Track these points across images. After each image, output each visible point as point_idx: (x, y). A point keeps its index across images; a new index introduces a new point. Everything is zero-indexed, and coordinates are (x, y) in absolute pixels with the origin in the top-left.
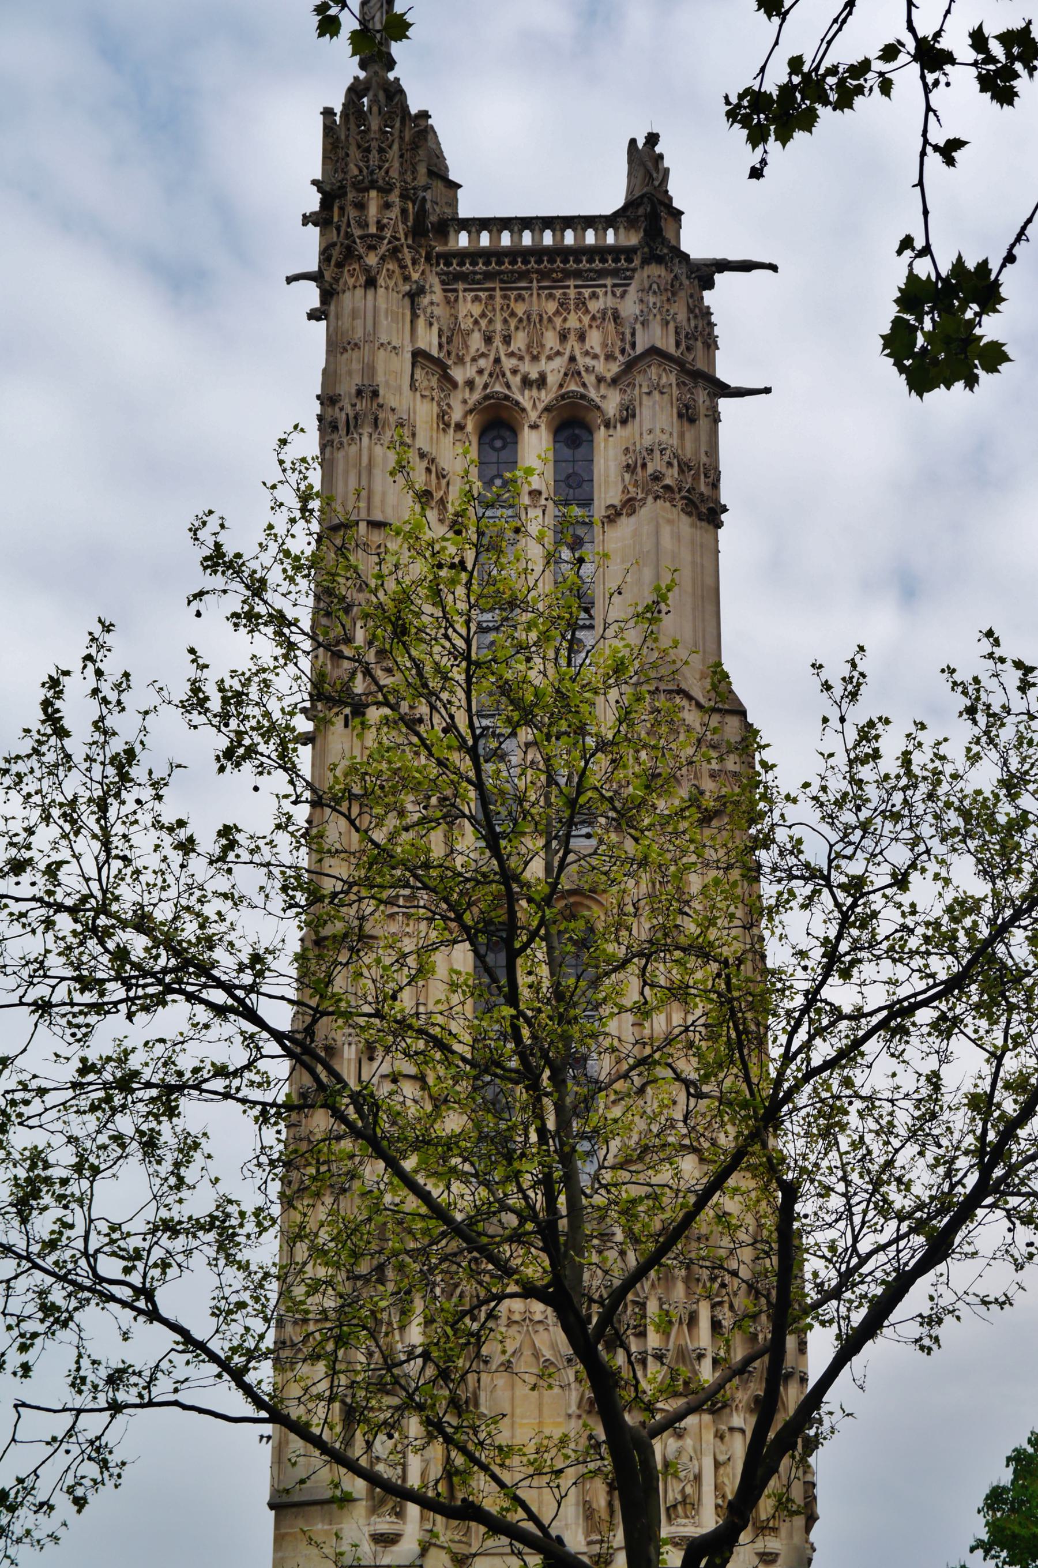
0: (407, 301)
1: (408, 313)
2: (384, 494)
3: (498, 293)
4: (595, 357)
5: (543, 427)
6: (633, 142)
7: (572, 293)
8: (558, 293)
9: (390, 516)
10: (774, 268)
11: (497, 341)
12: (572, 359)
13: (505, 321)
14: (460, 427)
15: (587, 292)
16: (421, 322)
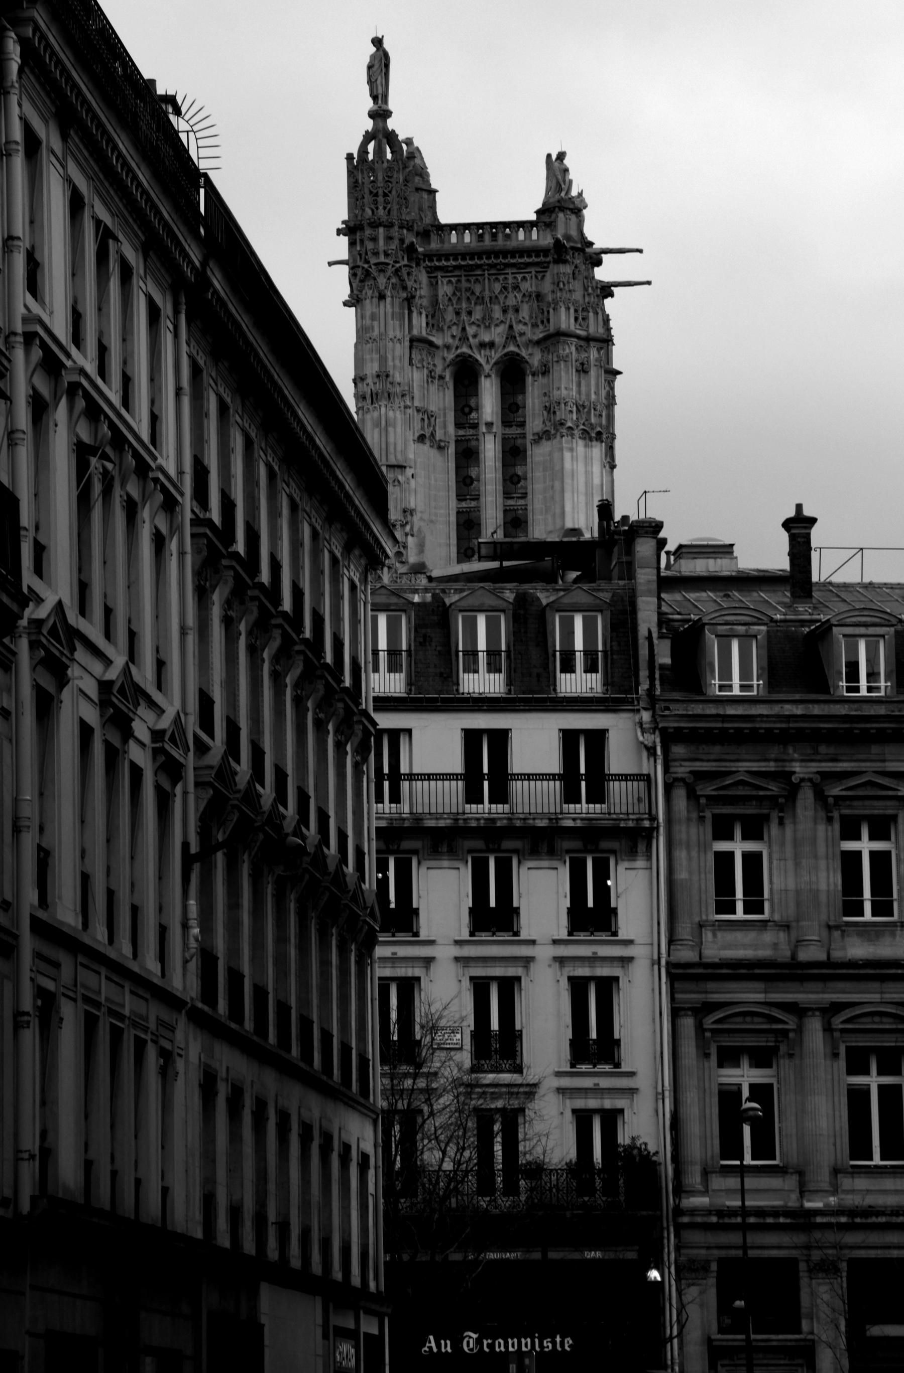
0: (406, 303)
1: (406, 312)
2: (395, 444)
3: (463, 278)
4: (525, 324)
5: (493, 376)
6: (549, 156)
7: (510, 281)
8: (501, 278)
9: (400, 460)
10: (640, 251)
11: (464, 316)
12: (511, 327)
13: (468, 298)
14: (441, 377)
15: (519, 277)
16: (415, 315)
